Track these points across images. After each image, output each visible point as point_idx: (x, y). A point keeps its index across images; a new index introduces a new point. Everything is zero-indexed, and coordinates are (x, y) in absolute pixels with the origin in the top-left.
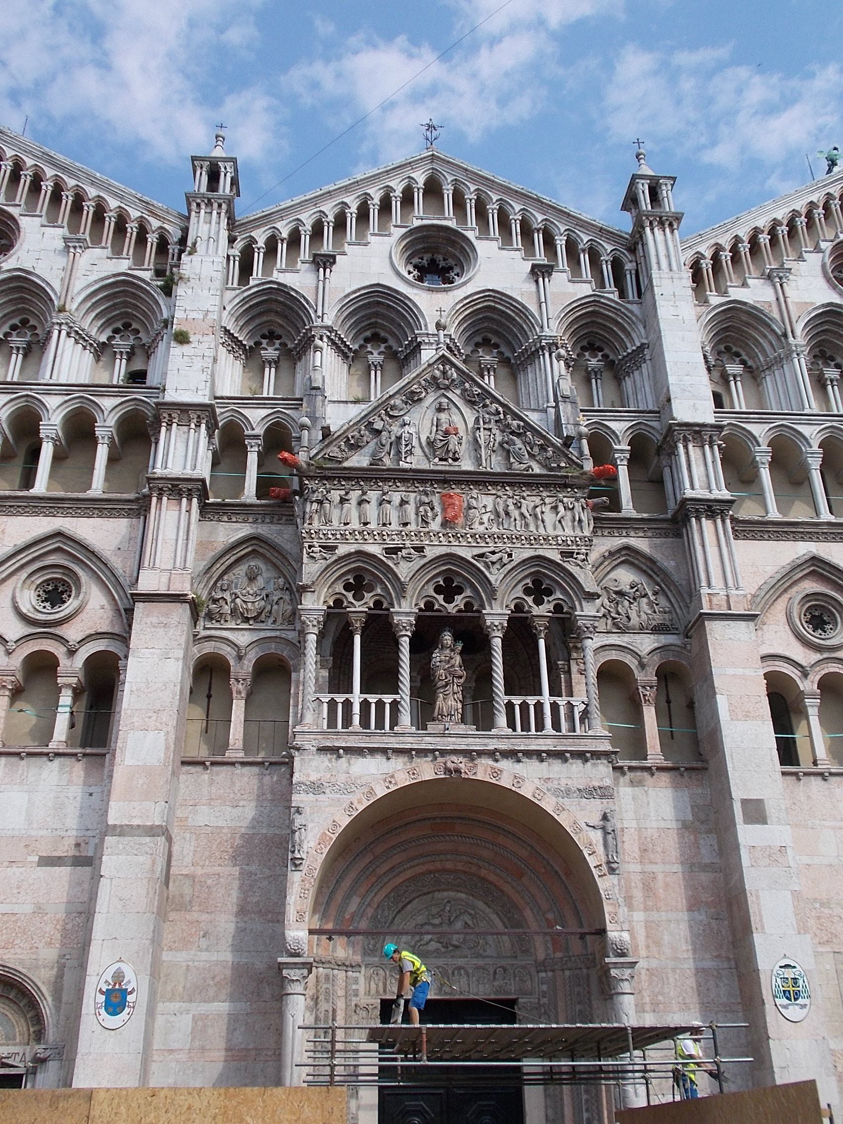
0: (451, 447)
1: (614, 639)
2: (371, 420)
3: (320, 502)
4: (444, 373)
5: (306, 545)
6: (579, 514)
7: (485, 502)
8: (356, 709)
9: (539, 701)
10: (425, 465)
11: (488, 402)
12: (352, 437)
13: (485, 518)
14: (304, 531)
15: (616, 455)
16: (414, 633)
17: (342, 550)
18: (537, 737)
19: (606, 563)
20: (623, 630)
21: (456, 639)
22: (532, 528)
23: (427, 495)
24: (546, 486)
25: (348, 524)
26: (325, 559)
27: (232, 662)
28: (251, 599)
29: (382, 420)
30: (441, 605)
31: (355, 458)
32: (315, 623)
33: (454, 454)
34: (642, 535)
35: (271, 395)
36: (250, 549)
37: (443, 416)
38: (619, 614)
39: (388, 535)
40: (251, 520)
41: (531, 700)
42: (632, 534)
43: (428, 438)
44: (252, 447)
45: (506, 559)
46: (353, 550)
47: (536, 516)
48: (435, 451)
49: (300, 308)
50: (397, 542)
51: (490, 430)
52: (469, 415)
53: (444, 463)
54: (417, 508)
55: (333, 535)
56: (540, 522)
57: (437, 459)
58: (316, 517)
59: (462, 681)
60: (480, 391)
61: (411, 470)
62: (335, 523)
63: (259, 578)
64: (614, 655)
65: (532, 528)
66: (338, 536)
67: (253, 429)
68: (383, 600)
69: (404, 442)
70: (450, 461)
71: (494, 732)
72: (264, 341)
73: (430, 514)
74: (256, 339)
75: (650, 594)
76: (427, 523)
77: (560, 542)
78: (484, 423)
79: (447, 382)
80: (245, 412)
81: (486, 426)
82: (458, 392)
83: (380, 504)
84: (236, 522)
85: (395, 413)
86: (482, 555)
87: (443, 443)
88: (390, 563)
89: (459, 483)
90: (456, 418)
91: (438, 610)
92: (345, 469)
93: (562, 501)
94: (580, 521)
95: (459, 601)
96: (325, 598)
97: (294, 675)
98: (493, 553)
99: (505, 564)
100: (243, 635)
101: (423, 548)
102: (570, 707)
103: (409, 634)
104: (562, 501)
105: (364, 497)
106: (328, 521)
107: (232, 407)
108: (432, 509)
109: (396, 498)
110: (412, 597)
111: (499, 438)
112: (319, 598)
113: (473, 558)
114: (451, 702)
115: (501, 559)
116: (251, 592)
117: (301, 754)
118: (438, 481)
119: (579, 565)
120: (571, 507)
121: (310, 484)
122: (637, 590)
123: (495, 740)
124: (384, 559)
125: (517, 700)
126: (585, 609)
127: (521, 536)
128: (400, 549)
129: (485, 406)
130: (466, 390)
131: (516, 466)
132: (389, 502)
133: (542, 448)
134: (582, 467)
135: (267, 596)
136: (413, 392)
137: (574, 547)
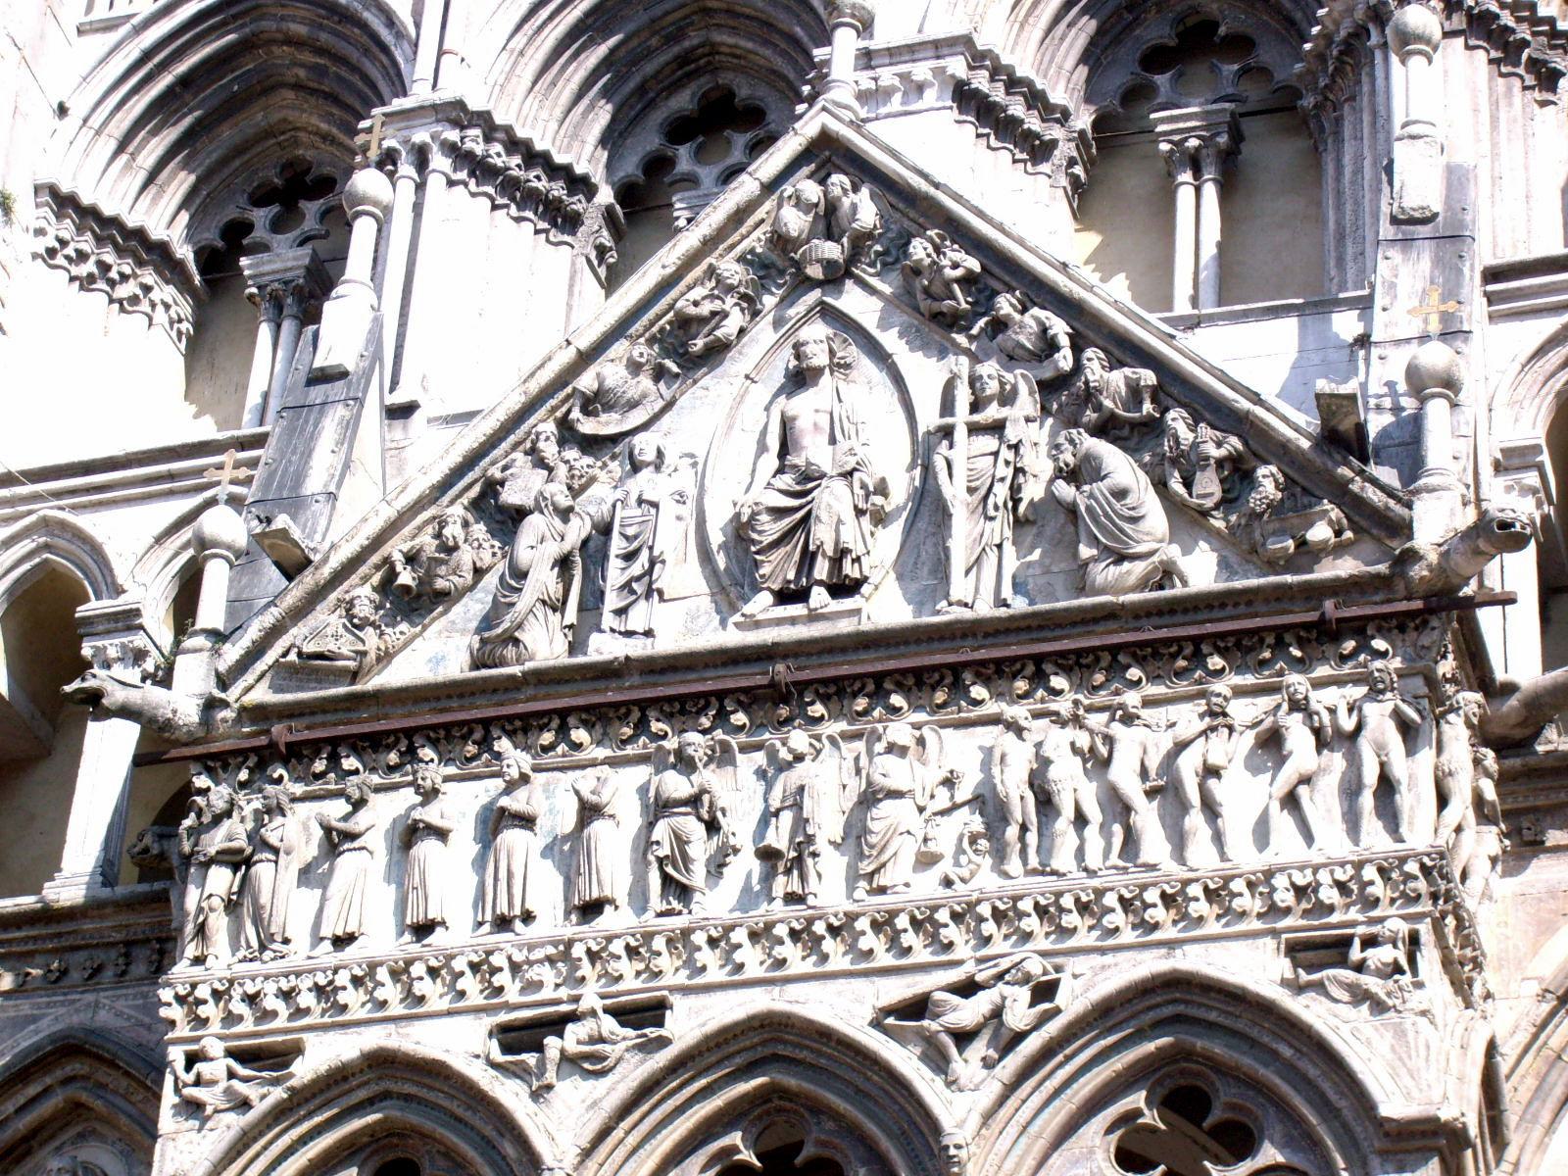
0: (822, 535)
2: (496, 472)
3: (237, 861)
5: (176, 1055)
11: (1005, 304)
14: (166, 995)
24: (1241, 648)
26: (244, 1105)
29: (541, 463)
37: (806, 406)
40: (76, 976)
45: (1019, 1012)
49: (366, 52)
51: (997, 428)
55: (287, 995)
56: (1195, 820)
60: (974, 264)
65: (1154, 845)
66: (307, 999)
70: (819, 596)
72: (261, 216)
74: (231, 213)
76: (684, 892)
77: (1284, 897)
79: (832, 250)
80: (86, 522)
86: (918, 1008)
87: (786, 522)
92: (379, 697)
93: (1297, 705)
94: (1387, 786)
99: (1019, 1037)
104: (1297, 705)
107: (48, 510)
113: (877, 1024)
115: (997, 1013)
127: (1100, 893)
130: (916, 271)
131: (1104, 573)
133: (1238, 474)
136: (686, 324)
137: (1354, 914)
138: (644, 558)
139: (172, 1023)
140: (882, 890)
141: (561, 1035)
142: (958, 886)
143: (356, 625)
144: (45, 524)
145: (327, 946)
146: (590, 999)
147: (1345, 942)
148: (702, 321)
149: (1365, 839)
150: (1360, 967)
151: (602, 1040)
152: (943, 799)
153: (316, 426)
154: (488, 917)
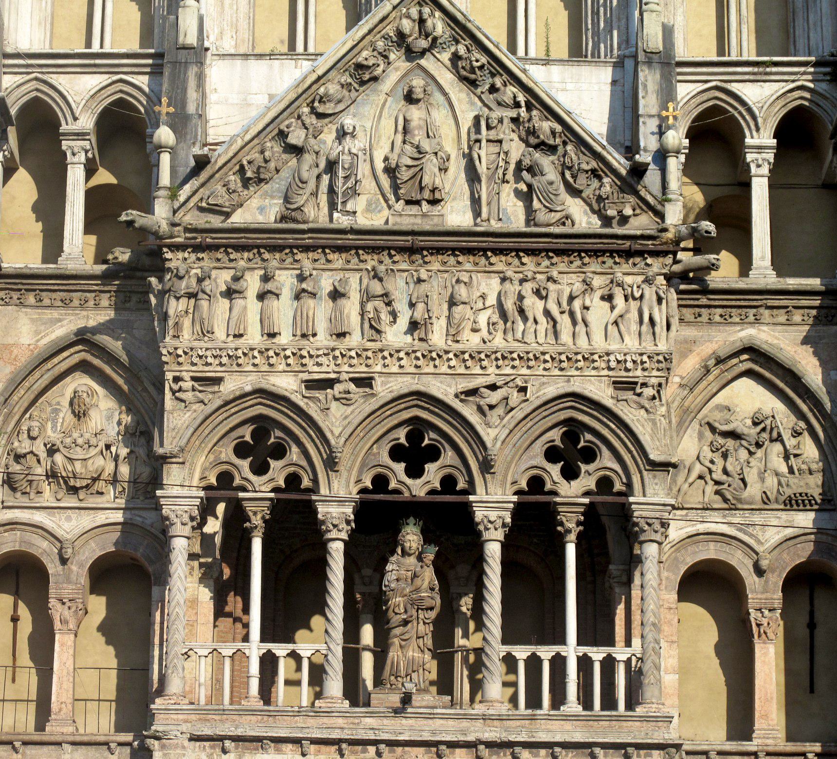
0: (426, 180)
1: (716, 523)
2: (282, 127)
4: (422, 21)
5: (169, 376)
6: (651, 309)
7: (483, 288)
8: (255, 668)
9: (558, 654)
10: (377, 220)
11: (498, 82)
12: (249, 162)
13: (483, 319)
14: (164, 352)
15: (749, 157)
16: (352, 534)
17: (232, 386)
18: (549, 718)
19: (711, 377)
20: (731, 505)
21: (428, 537)
22: (565, 337)
23: (376, 276)
24: (596, 253)
25: (241, 336)
26: (202, 402)
27: (53, 567)
28: (79, 453)
30: (400, 482)
31: (254, 203)
32: (186, 518)
33: (433, 191)
34: (782, 319)
35: (107, 49)
36: (76, 359)
37: (416, 114)
38: (725, 472)
39: (311, 356)
40: (76, 303)
41: (546, 653)
42: (767, 313)
43: (386, 159)
44: (74, 154)
45: (515, 398)
46: (248, 388)
47: (572, 314)
48: (395, 188)
50: (326, 369)
52: (465, 106)
53: (414, 209)
54: (362, 305)
56: (581, 328)
57: (402, 202)
58: (187, 323)
59: (433, 615)
61: (353, 231)
62: (220, 333)
63: (93, 413)
64: (711, 552)
66: (225, 360)
67: (75, 119)
68: (302, 472)
69: (341, 173)
71: (479, 709)
73: (385, 317)
75: (786, 436)
76: (378, 332)
77: (613, 364)
78: (489, 128)
81: (493, 135)
82: (446, 57)
83: (297, 297)
84: (51, 306)
85: (328, 108)
86: (473, 392)
88: (313, 410)
89: (438, 251)
90: (440, 116)
91: (397, 492)
94: (652, 321)
95: (433, 473)
96: (204, 470)
97: (155, 590)
98: (493, 387)
99: (512, 409)
100: (69, 519)
101: (372, 378)
102: (609, 664)
103: (344, 536)
105: (270, 286)
106: (206, 332)
108: (389, 304)
109: (326, 283)
110: (350, 471)
111: (514, 157)
112: (191, 475)
113: (456, 396)
114: (413, 653)
116: (80, 441)
117: (163, 747)
118: (401, 250)
119: (643, 407)
120: (637, 294)
121: (174, 260)
122: (764, 430)
123: (479, 724)
124: (302, 403)
125: (521, 653)
126: (649, 491)
128: (328, 384)
129: (493, 89)
131: (542, 216)
132: (313, 295)
134: (661, 216)
135: (108, 447)
138: (353, 180)
139: (167, 363)
140: (458, 341)
141: (332, 389)
142: (488, 343)
143: (230, 192)
144: (36, 79)
145: (231, 338)
146: (345, 376)
147: (636, 383)
148: (368, 67)
149: (644, 344)
150: (639, 395)
151: (349, 392)
152: (480, 305)
153: (185, 74)
154: (299, 333)
